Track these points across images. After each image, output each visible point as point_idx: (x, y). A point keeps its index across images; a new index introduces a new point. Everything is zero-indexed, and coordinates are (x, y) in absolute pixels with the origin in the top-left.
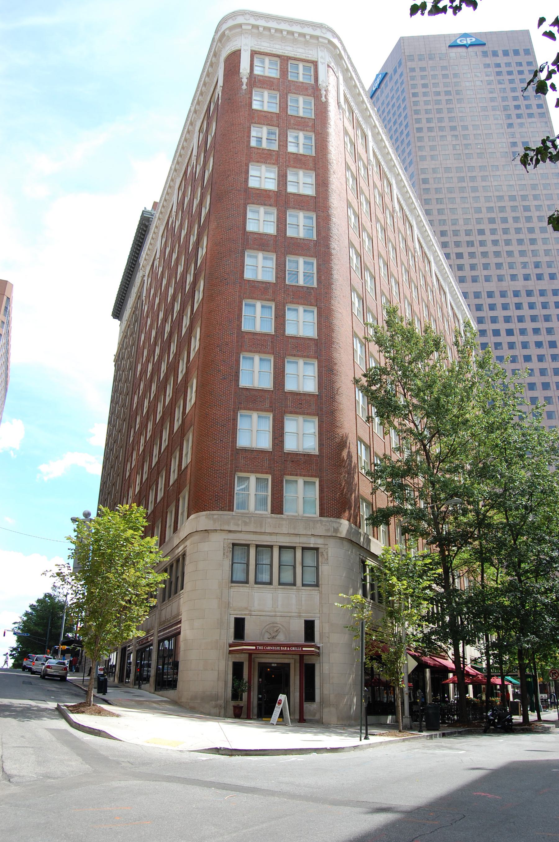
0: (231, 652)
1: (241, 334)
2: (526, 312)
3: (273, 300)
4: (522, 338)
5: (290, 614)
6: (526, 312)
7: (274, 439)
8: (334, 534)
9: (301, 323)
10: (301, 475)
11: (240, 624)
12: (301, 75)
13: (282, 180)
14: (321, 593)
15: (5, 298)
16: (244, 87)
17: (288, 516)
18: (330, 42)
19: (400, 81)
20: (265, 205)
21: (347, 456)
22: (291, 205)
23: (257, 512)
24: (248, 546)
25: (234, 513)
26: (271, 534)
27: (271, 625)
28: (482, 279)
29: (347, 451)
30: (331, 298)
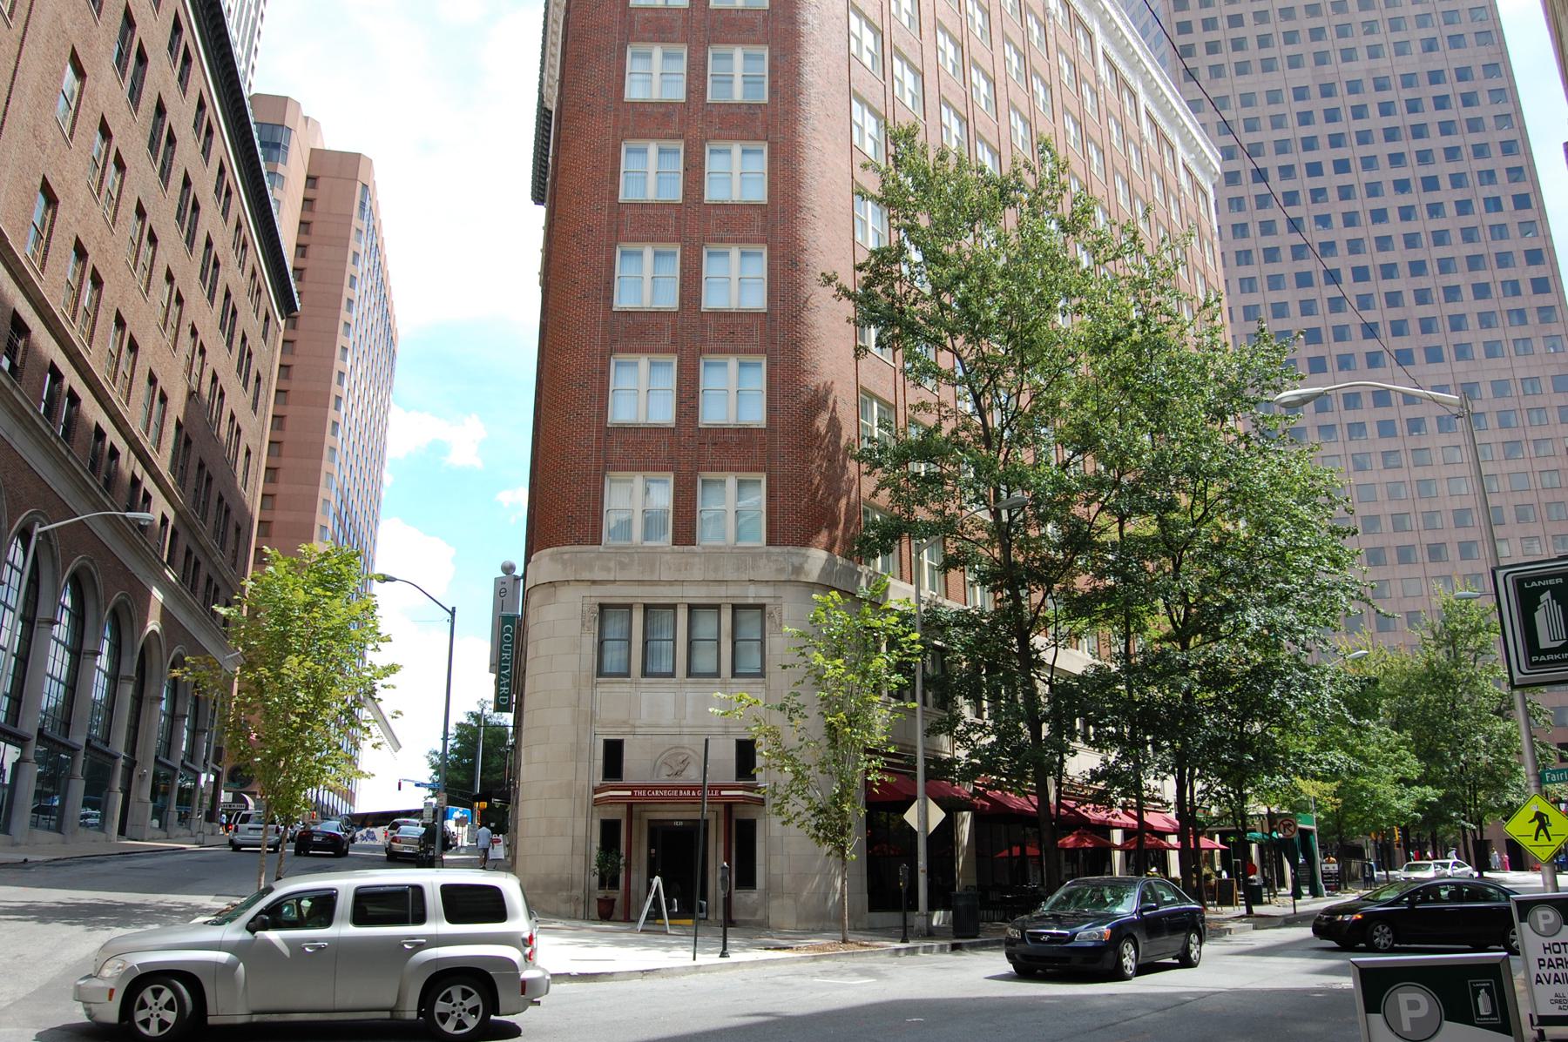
0: (596, 802)
1: (618, 209)
2: (1375, 122)
3: (680, 137)
4: (1367, 177)
7: (680, 402)
8: (793, 578)
9: (736, 176)
10: (731, 469)
11: (614, 751)
14: (767, 689)
21: (828, 426)
23: (647, 544)
24: (630, 607)
25: (601, 548)
26: (671, 583)
28: (1282, 63)
29: (827, 417)
30: (796, 121)
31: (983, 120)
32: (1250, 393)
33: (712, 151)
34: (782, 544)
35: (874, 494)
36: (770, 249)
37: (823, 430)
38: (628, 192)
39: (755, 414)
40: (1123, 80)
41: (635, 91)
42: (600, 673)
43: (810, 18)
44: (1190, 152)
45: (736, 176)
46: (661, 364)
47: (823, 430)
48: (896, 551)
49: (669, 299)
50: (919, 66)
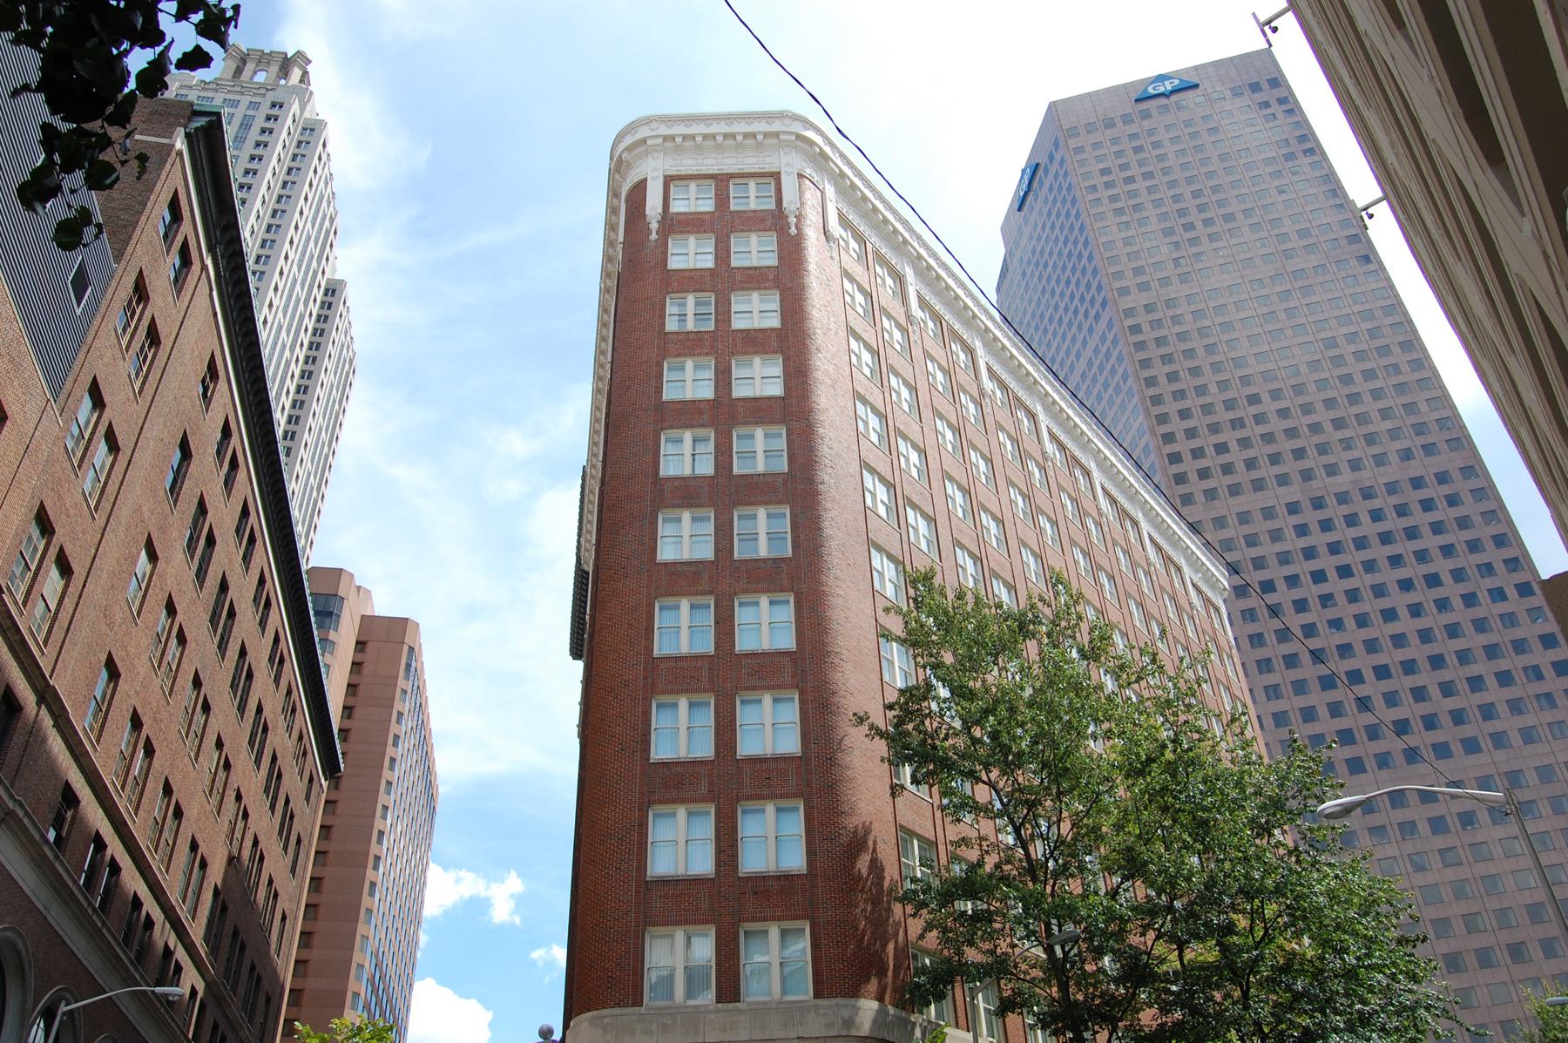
1: (653, 663)
2: (1368, 528)
3: (711, 592)
4: (1370, 579)
6: (1368, 528)
8: (844, 1032)
9: (765, 627)
10: (774, 919)
12: (751, 199)
13: (723, 379)
15: (406, 648)
16: (654, 236)
17: (749, 1004)
18: (799, 137)
19: (1061, 173)
20: (692, 426)
22: (740, 419)
23: (690, 1003)
25: (642, 1010)
29: (868, 858)
30: (819, 571)
31: (997, 559)
32: (1292, 804)
33: (741, 604)
34: (830, 996)
35: (922, 937)
36: (802, 694)
37: (864, 872)
38: (663, 646)
39: (795, 860)
40: (1124, 511)
41: (667, 552)
43: (826, 478)
44: (1197, 571)
45: (765, 627)
47: (864, 872)
48: (950, 997)
49: (704, 749)
50: (931, 513)
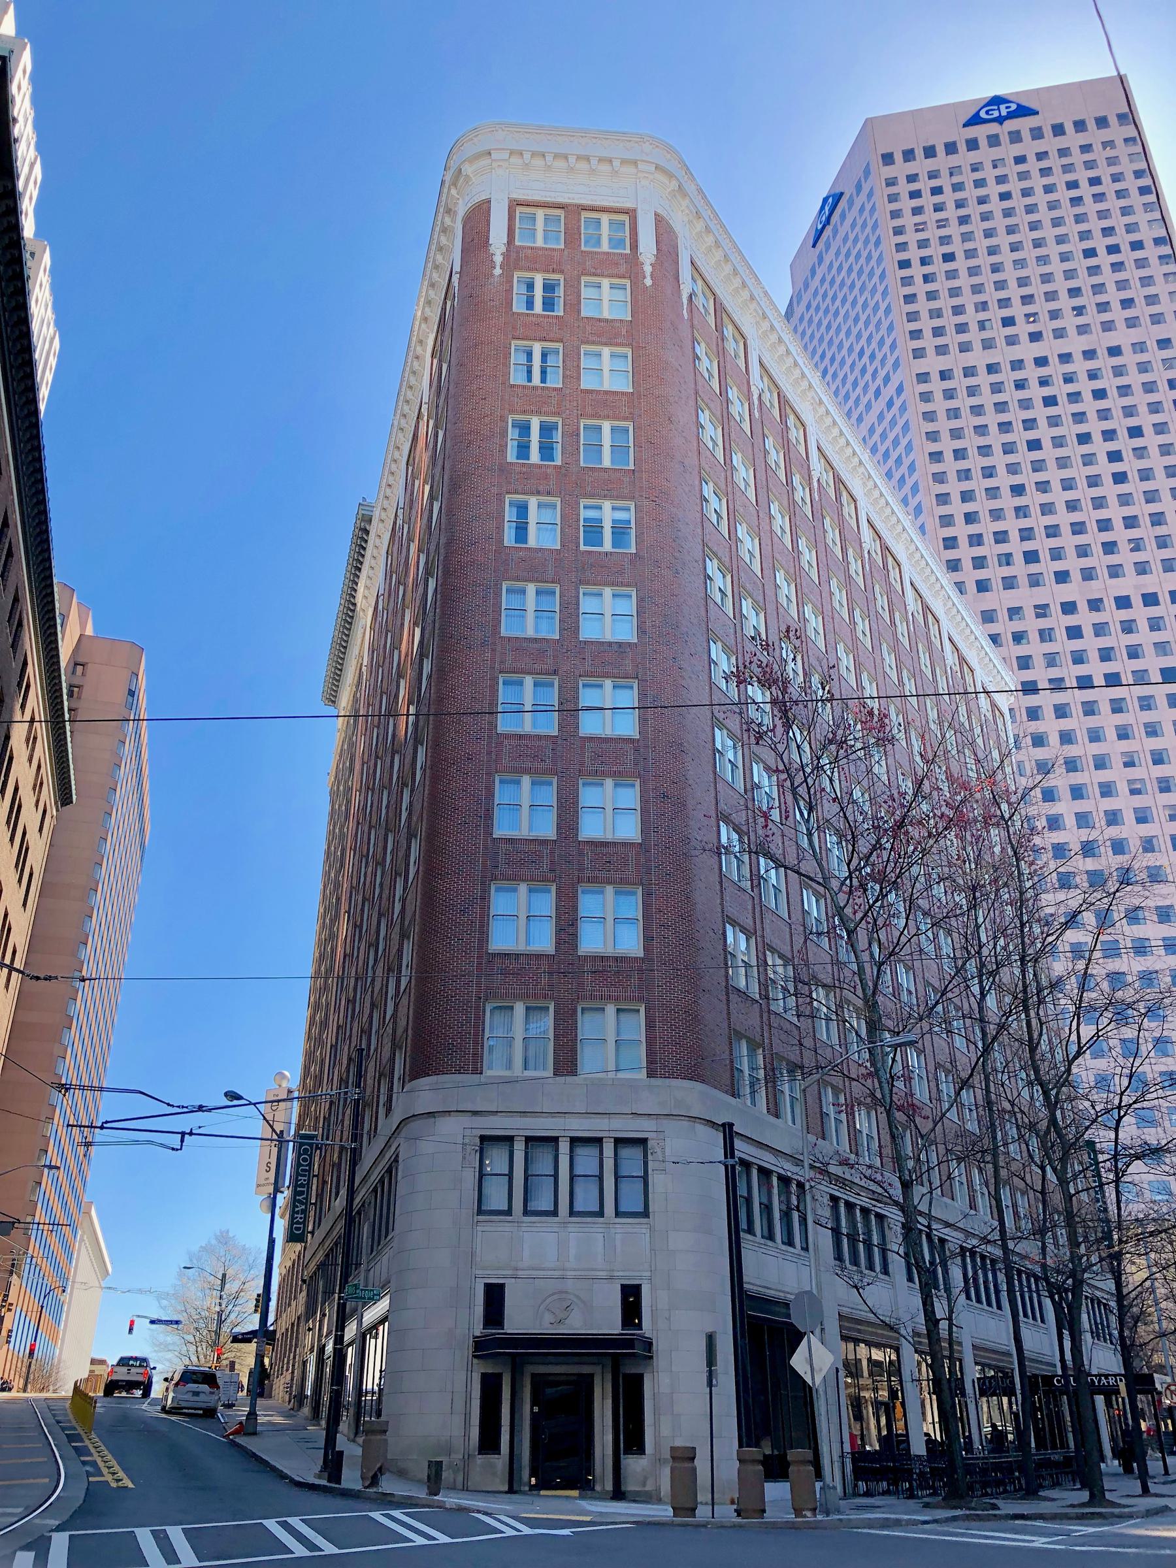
5: (593, 1273)
7: (560, 930)
11: (495, 1296)
16: (498, 271)
19: (868, 207)
20: (538, 493)
27: (556, 1297)
33: (584, 686)
39: (630, 943)
42: (480, 1212)
46: (536, 891)
